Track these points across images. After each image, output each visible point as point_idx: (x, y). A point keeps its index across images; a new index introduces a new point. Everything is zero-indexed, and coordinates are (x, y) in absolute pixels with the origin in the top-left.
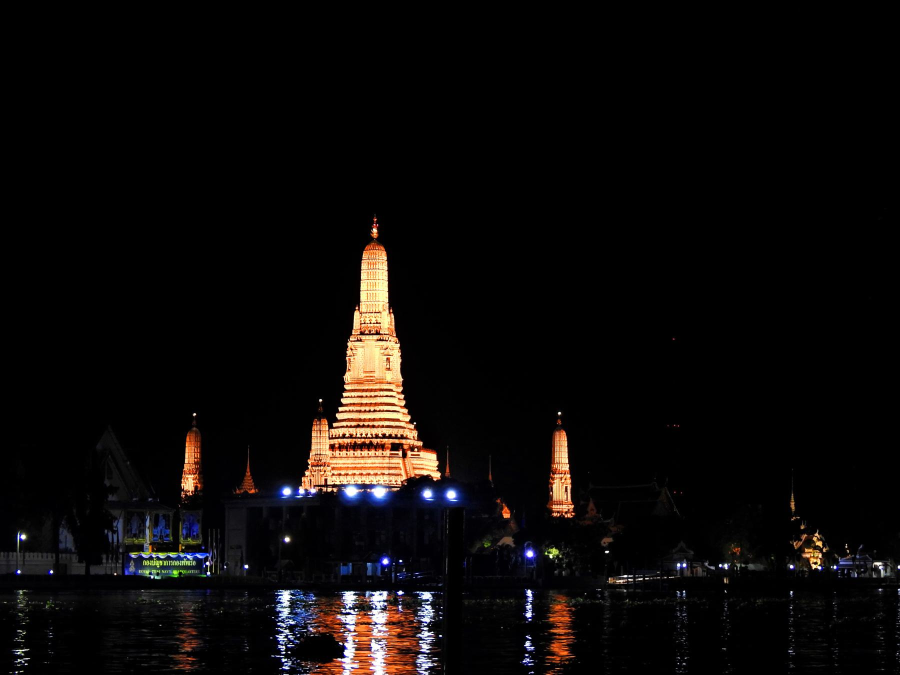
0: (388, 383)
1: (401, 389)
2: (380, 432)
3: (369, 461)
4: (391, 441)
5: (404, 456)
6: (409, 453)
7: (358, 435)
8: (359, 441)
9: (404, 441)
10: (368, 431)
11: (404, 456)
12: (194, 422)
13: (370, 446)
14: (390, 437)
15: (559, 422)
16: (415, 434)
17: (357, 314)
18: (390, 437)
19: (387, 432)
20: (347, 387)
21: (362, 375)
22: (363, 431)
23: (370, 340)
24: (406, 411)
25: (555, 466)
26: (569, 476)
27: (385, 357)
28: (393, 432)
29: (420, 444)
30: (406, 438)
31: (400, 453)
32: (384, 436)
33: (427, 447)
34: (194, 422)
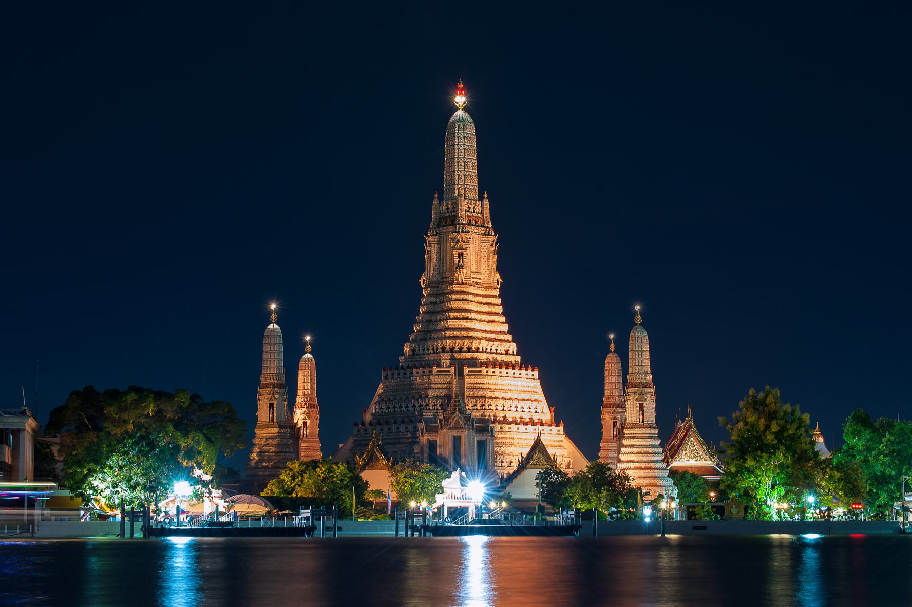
0: (458, 284)
1: (497, 293)
6: (466, 370)
7: (421, 352)
11: (460, 374)
12: (308, 348)
14: (452, 350)
15: (639, 319)
16: (513, 347)
17: (435, 202)
19: (449, 343)
24: (503, 319)
26: (653, 390)
27: (455, 253)
29: (519, 359)
31: (452, 370)
33: (525, 364)
34: (308, 348)
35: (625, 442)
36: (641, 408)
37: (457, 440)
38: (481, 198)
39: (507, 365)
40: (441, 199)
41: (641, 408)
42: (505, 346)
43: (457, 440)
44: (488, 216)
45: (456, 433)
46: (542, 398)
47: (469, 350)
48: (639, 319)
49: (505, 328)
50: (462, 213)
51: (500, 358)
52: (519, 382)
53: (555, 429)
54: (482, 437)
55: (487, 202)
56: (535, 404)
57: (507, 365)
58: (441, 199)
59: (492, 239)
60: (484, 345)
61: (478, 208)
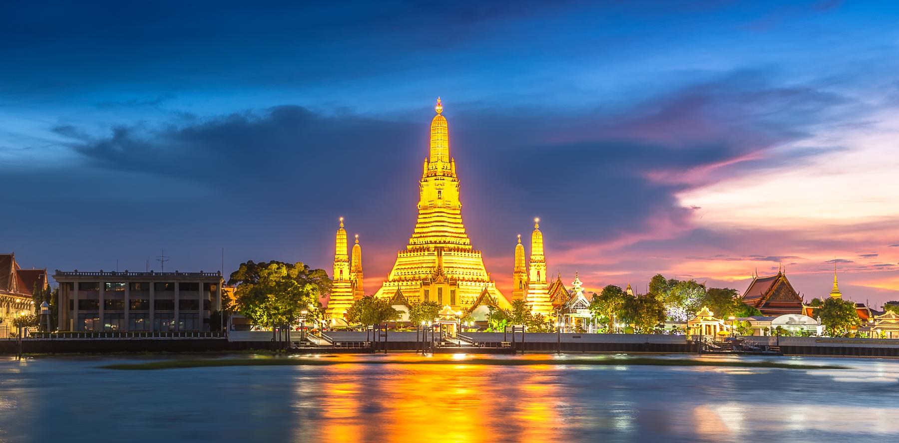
1: (458, 212)
2: (429, 239)
3: (418, 258)
4: (433, 245)
5: (440, 255)
6: (443, 253)
8: (418, 247)
9: (444, 245)
10: (439, 239)
11: (440, 255)
13: (421, 250)
14: (435, 243)
15: (537, 226)
16: (468, 241)
17: (426, 164)
18: (435, 243)
20: (421, 212)
21: (428, 204)
22: (421, 240)
23: (432, 180)
25: (532, 257)
28: (438, 239)
30: (449, 243)
31: (436, 253)
32: (431, 242)
34: (357, 241)
35: (530, 291)
36: (538, 273)
37: (440, 290)
38: (450, 162)
39: (465, 250)
40: (429, 162)
41: (538, 273)
42: (463, 240)
43: (440, 290)
44: (454, 172)
45: (440, 286)
46: (483, 268)
47: (445, 242)
48: (537, 226)
49: (463, 231)
50: (439, 170)
51: (460, 246)
52: (470, 259)
53: (490, 284)
54: (453, 288)
55: (453, 164)
56: (479, 271)
57: (465, 250)
58: (429, 162)
59: (456, 183)
60: (452, 240)
61: (449, 167)
